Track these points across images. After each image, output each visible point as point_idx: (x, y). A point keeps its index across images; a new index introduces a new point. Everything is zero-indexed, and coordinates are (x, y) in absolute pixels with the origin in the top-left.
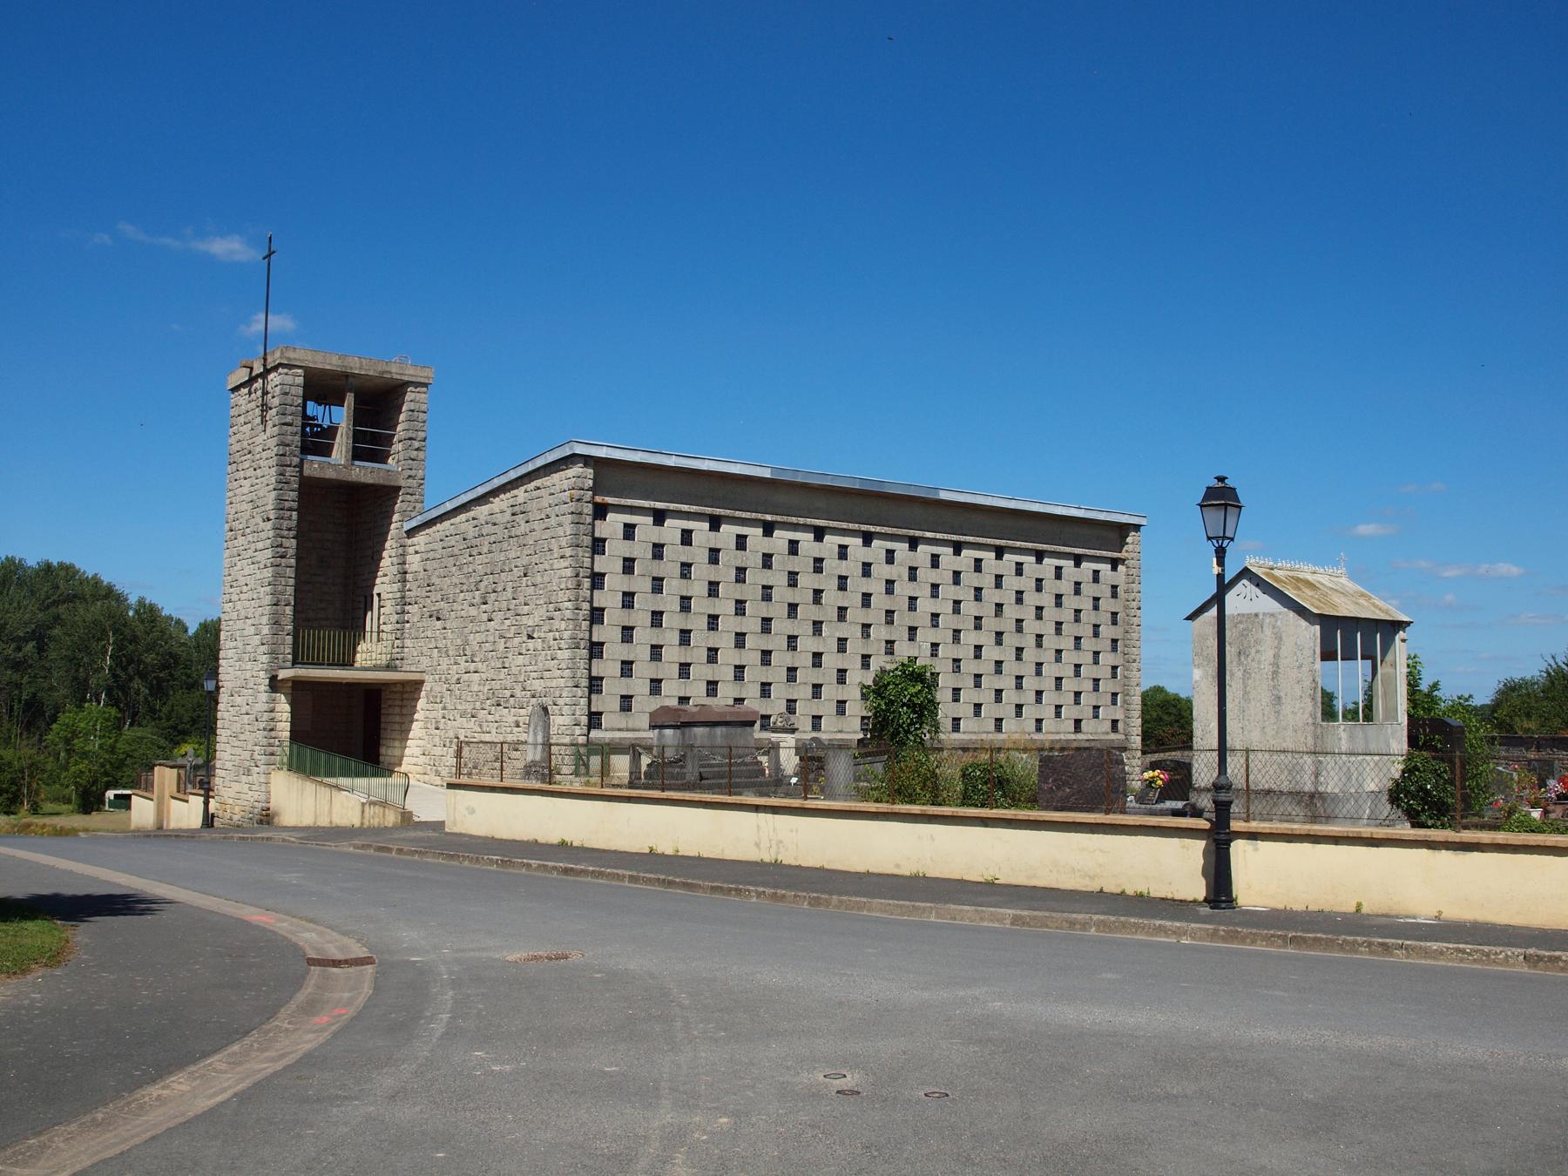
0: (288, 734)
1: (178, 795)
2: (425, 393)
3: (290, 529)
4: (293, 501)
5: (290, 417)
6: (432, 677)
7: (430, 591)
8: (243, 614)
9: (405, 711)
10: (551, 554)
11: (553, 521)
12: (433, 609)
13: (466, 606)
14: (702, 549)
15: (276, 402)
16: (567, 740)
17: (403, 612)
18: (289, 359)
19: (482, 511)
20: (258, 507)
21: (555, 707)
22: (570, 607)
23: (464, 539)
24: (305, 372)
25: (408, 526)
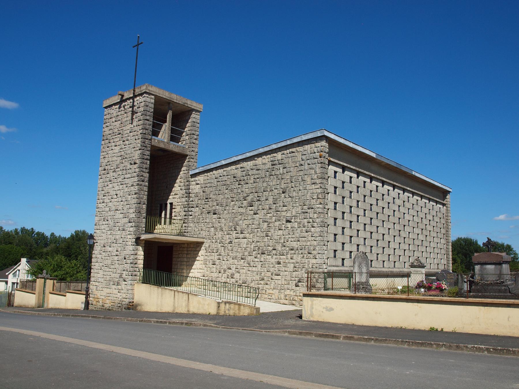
0: (142, 266)
1: (53, 292)
2: (199, 115)
3: (146, 169)
5: (148, 117)
7: (208, 201)
8: (114, 208)
9: (189, 256)
13: (236, 208)
18: (149, 90)
19: (248, 165)
21: (309, 255)
22: (321, 207)
23: (234, 177)
25: (191, 173)
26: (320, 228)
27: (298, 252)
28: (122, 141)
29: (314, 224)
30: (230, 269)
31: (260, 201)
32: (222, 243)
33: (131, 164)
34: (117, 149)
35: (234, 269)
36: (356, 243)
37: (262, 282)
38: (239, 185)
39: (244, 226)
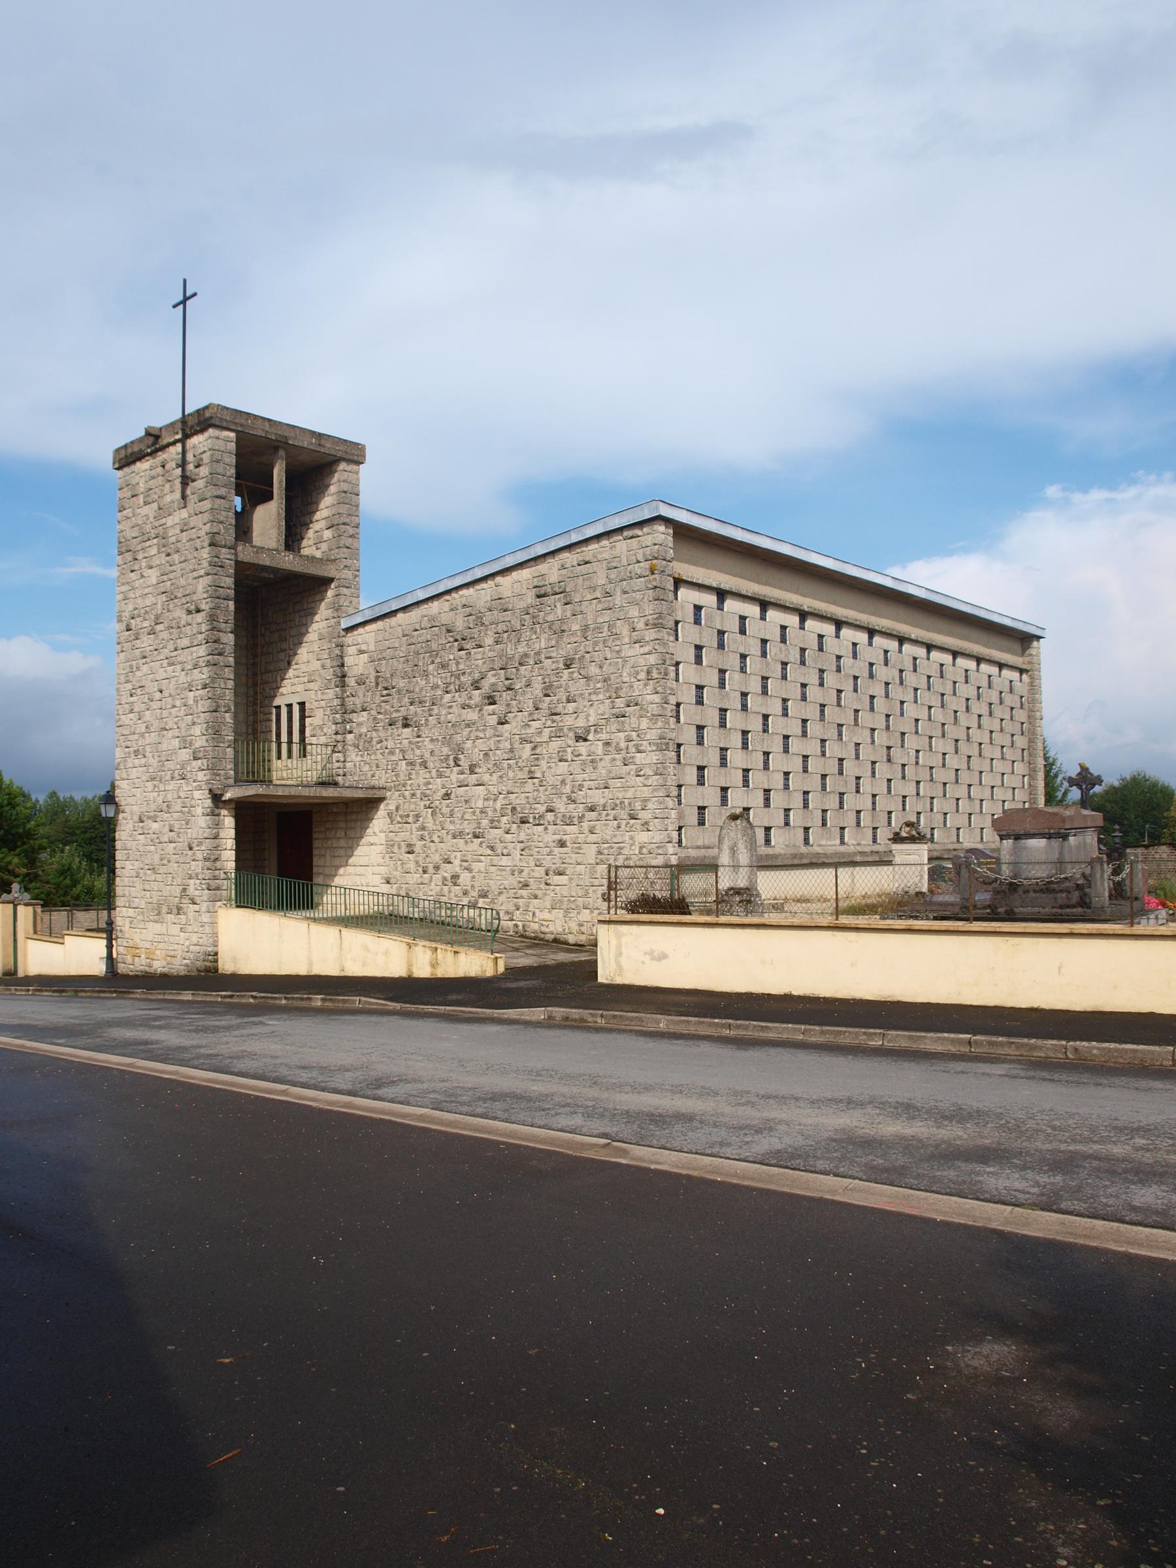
4: (228, 588)
6: (397, 793)
7: (388, 695)
8: (156, 725)
10: (618, 639)
11: (618, 599)
12: (395, 715)
13: (456, 710)
15: (204, 471)
16: (660, 861)
17: (344, 721)
19: (481, 596)
20: (176, 597)
21: (632, 821)
23: (449, 631)
25: (345, 623)
26: (657, 753)
27: (607, 815)
28: (164, 554)
29: (641, 745)
30: (450, 862)
31: (513, 689)
32: (426, 799)
33: (189, 612)
34: (153, 576)
35: (457, 862)
36: (760, 786)
37: (524, 893)
38: (459, 650)
39: (477, 756)
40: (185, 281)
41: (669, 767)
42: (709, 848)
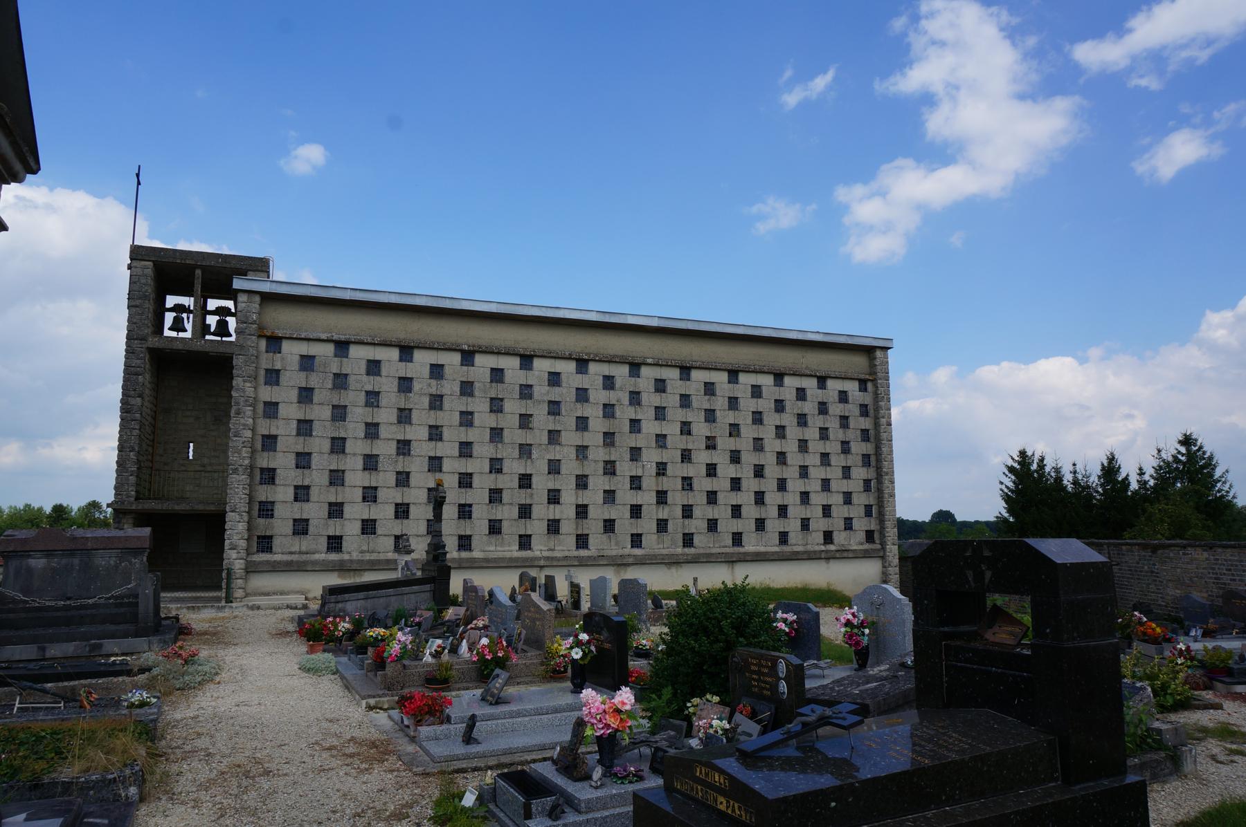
14: (390, 379)
24: (154, 265)
36: (390, 501)
40: (139, 166)
41: (237, 488)
42: (307, 553)
